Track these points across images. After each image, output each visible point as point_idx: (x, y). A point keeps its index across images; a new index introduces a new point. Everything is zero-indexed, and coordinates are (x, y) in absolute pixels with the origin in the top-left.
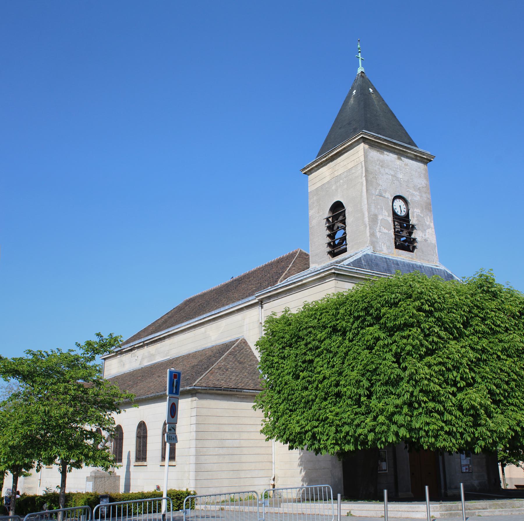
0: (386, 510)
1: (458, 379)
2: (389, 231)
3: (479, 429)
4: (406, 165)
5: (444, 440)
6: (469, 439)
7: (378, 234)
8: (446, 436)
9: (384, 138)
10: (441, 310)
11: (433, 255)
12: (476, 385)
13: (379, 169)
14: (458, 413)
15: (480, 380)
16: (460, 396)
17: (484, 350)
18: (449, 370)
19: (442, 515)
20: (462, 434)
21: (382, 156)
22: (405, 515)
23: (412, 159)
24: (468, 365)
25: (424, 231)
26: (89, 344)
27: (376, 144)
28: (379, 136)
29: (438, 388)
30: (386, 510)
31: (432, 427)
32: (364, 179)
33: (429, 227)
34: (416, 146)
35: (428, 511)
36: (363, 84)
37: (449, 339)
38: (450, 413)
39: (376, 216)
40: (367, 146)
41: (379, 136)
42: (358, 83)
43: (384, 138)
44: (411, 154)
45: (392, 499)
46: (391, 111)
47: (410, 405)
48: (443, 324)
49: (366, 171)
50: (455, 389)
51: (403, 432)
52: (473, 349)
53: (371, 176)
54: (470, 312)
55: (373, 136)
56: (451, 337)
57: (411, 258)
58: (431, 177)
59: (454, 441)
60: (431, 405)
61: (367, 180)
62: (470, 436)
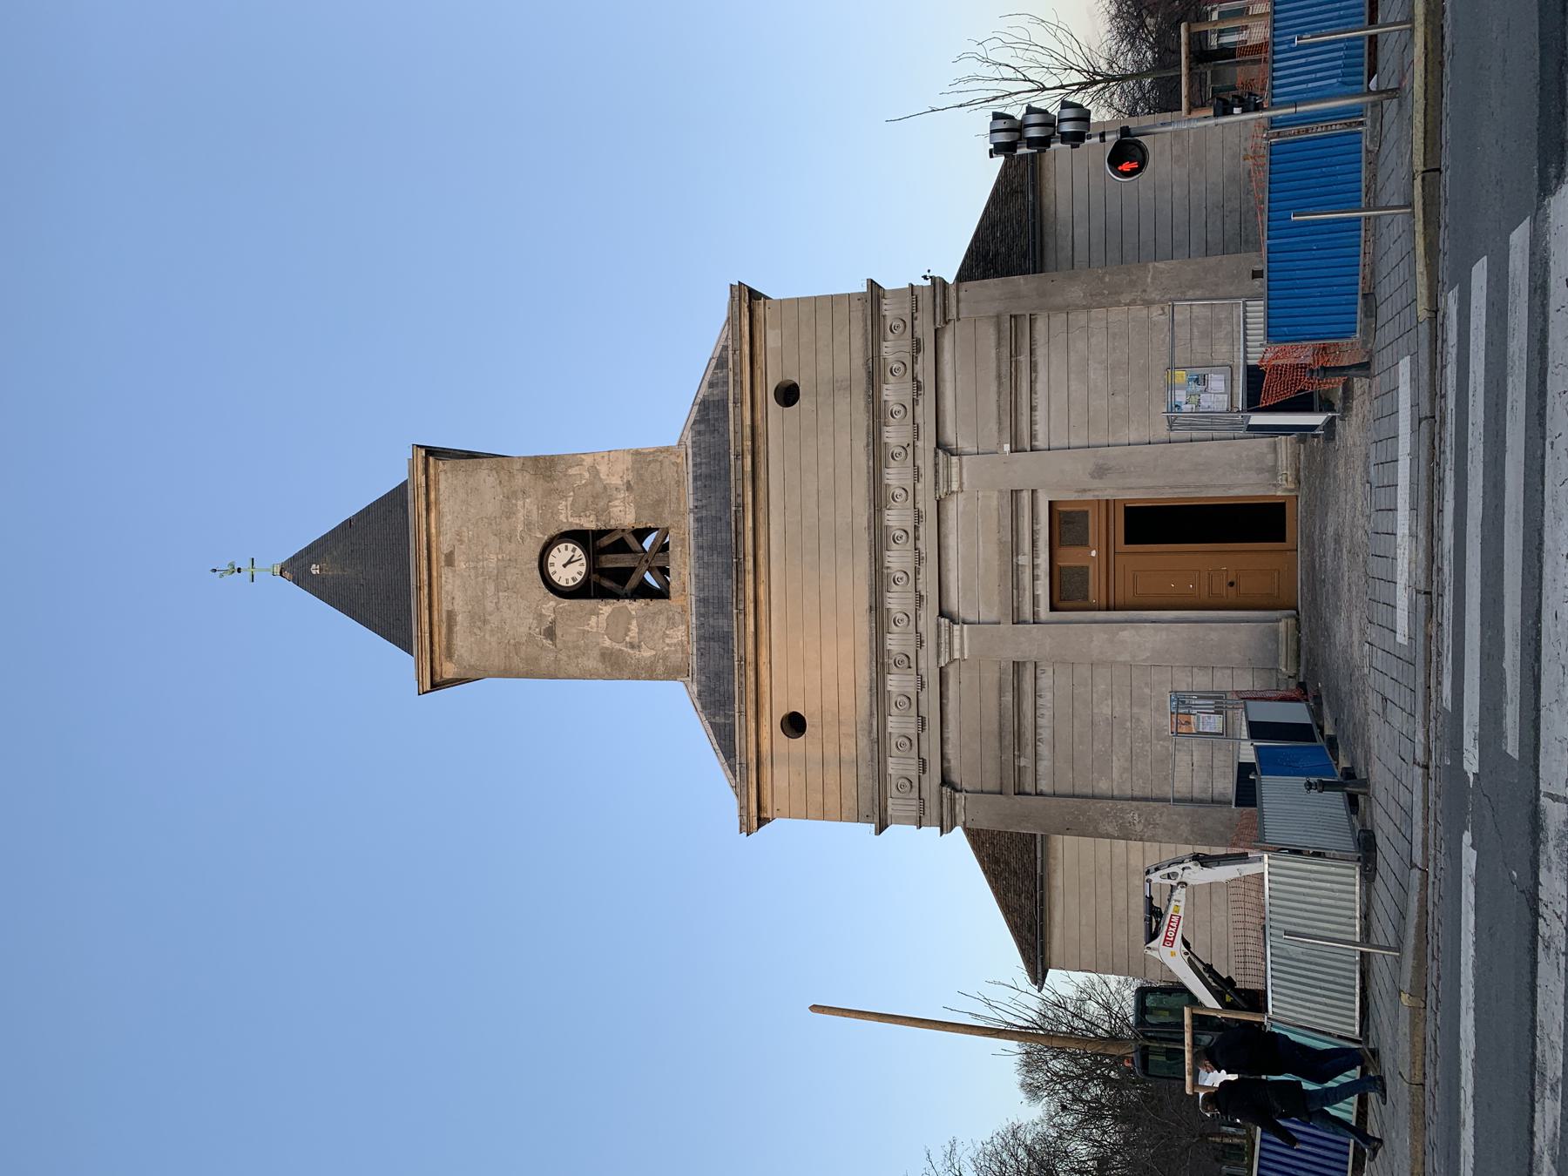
2: (630, 617)
7: (647, 653)
39: (606, 655)
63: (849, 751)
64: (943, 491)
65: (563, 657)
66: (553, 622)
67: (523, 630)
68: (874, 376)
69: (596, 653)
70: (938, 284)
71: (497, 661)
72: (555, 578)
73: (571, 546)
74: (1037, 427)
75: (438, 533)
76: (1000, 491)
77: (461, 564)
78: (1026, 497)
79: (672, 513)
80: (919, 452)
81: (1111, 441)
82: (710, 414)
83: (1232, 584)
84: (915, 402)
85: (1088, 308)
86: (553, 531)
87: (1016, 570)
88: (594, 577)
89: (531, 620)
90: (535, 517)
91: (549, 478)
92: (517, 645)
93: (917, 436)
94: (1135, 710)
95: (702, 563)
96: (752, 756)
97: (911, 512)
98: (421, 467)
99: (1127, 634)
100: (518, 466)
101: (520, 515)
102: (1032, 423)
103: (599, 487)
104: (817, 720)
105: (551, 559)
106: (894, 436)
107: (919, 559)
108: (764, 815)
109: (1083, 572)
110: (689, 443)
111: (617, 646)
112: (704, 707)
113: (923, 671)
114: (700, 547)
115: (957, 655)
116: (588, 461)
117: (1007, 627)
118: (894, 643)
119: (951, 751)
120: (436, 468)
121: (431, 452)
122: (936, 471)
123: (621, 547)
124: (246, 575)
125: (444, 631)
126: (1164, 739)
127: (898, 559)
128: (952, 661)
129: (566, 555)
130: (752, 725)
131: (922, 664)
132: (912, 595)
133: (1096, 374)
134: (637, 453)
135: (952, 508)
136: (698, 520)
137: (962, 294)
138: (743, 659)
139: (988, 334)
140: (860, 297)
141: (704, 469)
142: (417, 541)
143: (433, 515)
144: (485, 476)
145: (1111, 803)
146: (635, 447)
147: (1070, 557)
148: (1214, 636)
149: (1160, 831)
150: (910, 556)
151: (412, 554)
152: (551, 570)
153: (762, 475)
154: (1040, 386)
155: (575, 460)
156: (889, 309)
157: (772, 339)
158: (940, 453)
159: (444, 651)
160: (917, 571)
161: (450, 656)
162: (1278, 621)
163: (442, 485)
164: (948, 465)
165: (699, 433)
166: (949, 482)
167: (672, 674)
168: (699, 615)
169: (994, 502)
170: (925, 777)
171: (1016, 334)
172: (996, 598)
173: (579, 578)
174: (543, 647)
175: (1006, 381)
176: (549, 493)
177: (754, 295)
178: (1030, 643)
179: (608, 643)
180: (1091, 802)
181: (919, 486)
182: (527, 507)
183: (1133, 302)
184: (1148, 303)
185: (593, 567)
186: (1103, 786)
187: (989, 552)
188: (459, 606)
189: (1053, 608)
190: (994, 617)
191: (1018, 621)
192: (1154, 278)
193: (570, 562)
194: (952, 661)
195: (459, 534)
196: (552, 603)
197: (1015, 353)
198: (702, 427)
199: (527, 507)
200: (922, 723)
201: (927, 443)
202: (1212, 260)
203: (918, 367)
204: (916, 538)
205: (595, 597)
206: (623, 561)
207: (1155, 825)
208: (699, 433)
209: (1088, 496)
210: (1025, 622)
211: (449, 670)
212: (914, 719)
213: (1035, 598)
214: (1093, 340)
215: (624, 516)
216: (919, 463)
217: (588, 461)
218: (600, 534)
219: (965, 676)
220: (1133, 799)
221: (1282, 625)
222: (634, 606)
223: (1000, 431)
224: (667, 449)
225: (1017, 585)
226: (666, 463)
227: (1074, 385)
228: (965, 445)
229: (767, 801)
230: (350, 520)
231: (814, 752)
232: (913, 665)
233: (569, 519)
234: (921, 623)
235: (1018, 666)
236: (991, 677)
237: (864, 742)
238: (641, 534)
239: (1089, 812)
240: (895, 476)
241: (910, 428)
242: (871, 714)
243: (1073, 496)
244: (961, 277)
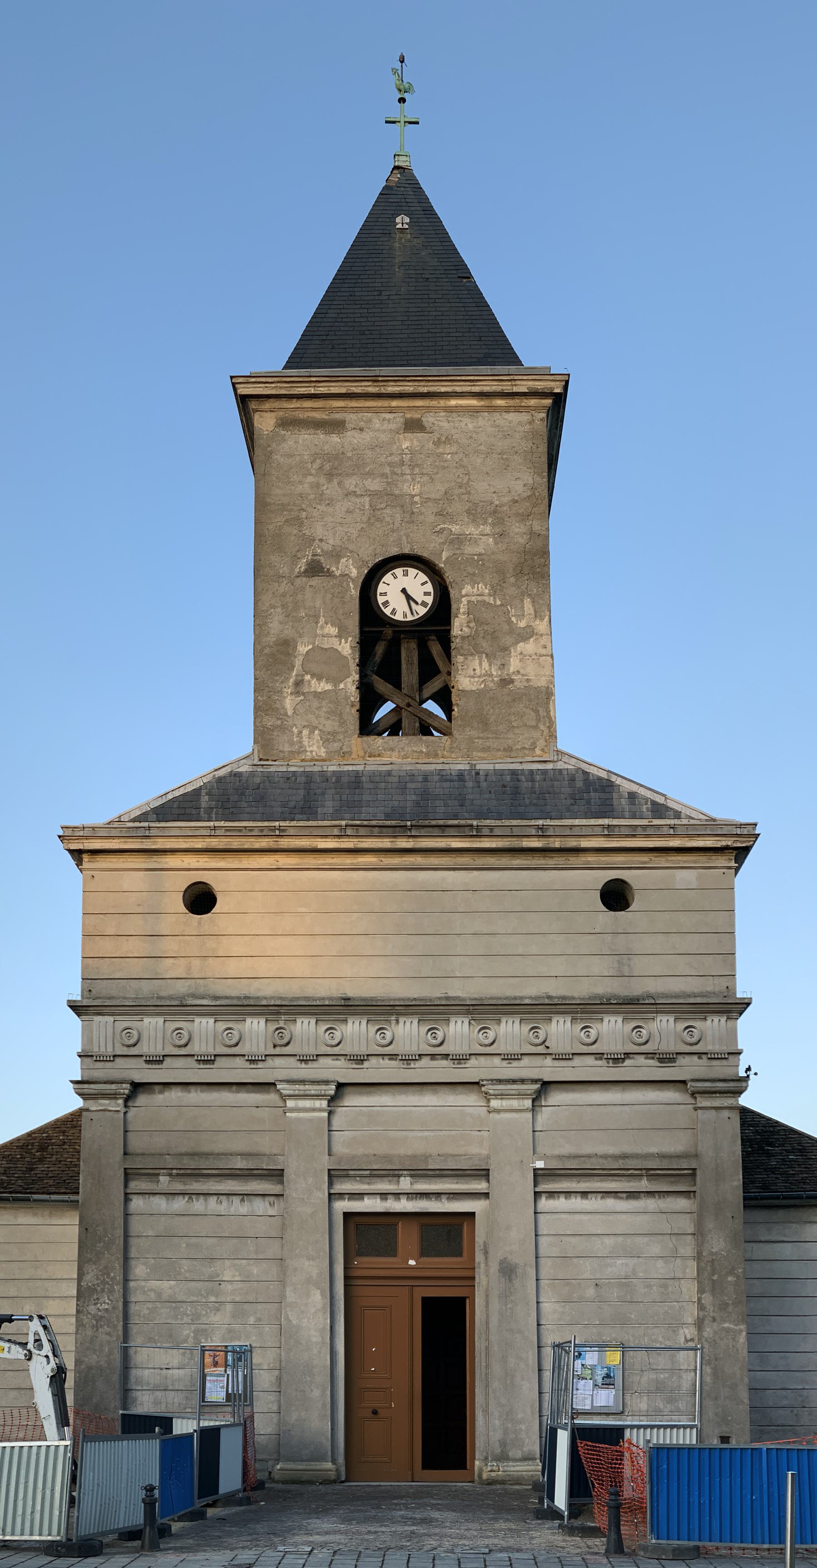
2: (336, 681)
7: (289, 703)
11: (536, 727)
13: (318, 485)
23: (474, 412)
39: (286, 646)
53: (279, 520)
57: (428, 755)
63: (172, 968)
64: (491, 1089)
65: (284, 587)
66: (329, 574)
67: (319, 531)
68: (633, 1006)
69: (289, 632)
70: (738, 1085)
71: (278, 493)
72: (388, 577)
73: (430, 600)
74: (562, 1199)
75: (449, 410)
76: (488, 1157)
77: (407, 442)
78: (480, 1186)
79: (471, 740)
80: (538, 1061)
81: (543, 1283)
82: (596, 794)
83: (375, 1412)
84: (599, 1056)
85: (699, 1257)
86: (450, 576)
87: (394, 1174)
88: (389, 632)
89: (332, 541)
90: (469, 549)
91: (519, 572)
92: (298, 522)
93: (558, 1057)
94: (229, 1307)
95: (404, 781)
96: (160, 844)
97: (466, 1050)
98: (540, 385)
99: (317, 1298)
100: (537, 527)
101: (471, 530)
102: (568, 1194)
104: (206, 929)
105: (412, 571)
106: (560, 1030)
107: (408, 1060)
108: (86, 858)
109: (390, 1250)
110: (560, 765)
111: (298, 663)
112: (220, 780)
113: (270, 1062)
114: (426, 777)
115: (290, 1103)
116: (541, 626)
117: (325, 1163)
118: (304, 1028)
119: (174, 1095)
120: (536, 409)
121: (559, 401)
122: (514, 1081)
123: (428, 669)
124: (395, 111)
125: (317, 415)
126: (195, 1338)
127: (408, 1032)
128: (284, 1098)
129: (417, 593)
130: (199, 844)
131: (278, 1061)
132: (364, 1050)
133: (620, 1266)
134: (548, 694)
135: (469, 1100)
136: (461, 775)
137: (726, 1114)
138: (282, 833)
139: (675, 1144)
140: (730, 990)
141: (525, 785)
142: (440, 379)
143: (474, 402)
144: (522, 480)
145: (120, 1278)
146: (558, 691)
147: (408, 1237)
148: (316, 1393)
149: (89, 1333)
150: (412, 1049)
151: (420, 370)
152: (399, 571)
153: (518, 862)
154: (611, 1203)
155: (543, 608)
156: (714, 1024)
157: (686, 876)
158: (537, 1086)
159: (289, 415)
160: (392, 1057)
161: (285, 423)
162: (334, 1461)
163: (513, 417)
164: (521, 1095)
165: (572, 779)
166: (501, 1096)
167: (262, 736)
168: (338, 775)
169: (474, 1150)
170: (140, 1063)
171: (674, 1175)
172: (360, 1151)
173: (387, 611)
174: (295, 558)
175: (620, 1164)
176: (500, 571)
177: (741, 854)
178: (307, 1191)
179: (303, 649)
180: (120, 1256)
181: (497, 1061)
182: (482, 539)
183: (701, 1307)
184: (699, 1324)
185: (403, 630)
186: (139, 1270)
187: (415, 1144)
188: (352, 439)
189: (347, 1216)
190: (338, 1148)
191: (333, 1176)
192: (728, 1330)
193: (409, 598)
194: (284, 1098)
195: (448, 440)
196: (354, 572)
197: (651, 1174)
198: (579, 784)
199: (482, 539)
200: (208, 1061)
201: (549, 1070)
202: (744, 1395)
203: (641, 1060)
204: (433, 1056)
205: (362, 632)
206: (409, 673)
207: (96, 1328)
208: (572, 779)
209: (479, 1257)
210: (331, 1184)
211: (265, 422)
212: (211, 1051)
213: (359, 1196)
214: (660, 1263)
215: (469, 675)
216: (526, 1061)
217: (541, 626)
218: (446, 641)
219: (264, 1113)
220: (126, 1304)
221: (329, 1465)
222: (350, 686)
223: (560, 1157)
224: (553, 736)
225: (375, 1175)
226: (536, 734)
227: (609, 1241)
228: (545, 1116)
229: (103, 862)
230: (469, 277)
231: (166, 925)
232: (278, 1051)
233: (467, 595)
234: (328, 1061)
235: (278, 1175)
236: (265, 1144)
237: (181, 988)
238: (444, 698)
239: (107, 1254)
240: (510, 1031)
241: (569, 1050)
242: (216, 998)
243: (480, 1239)
244: (745, 1112)
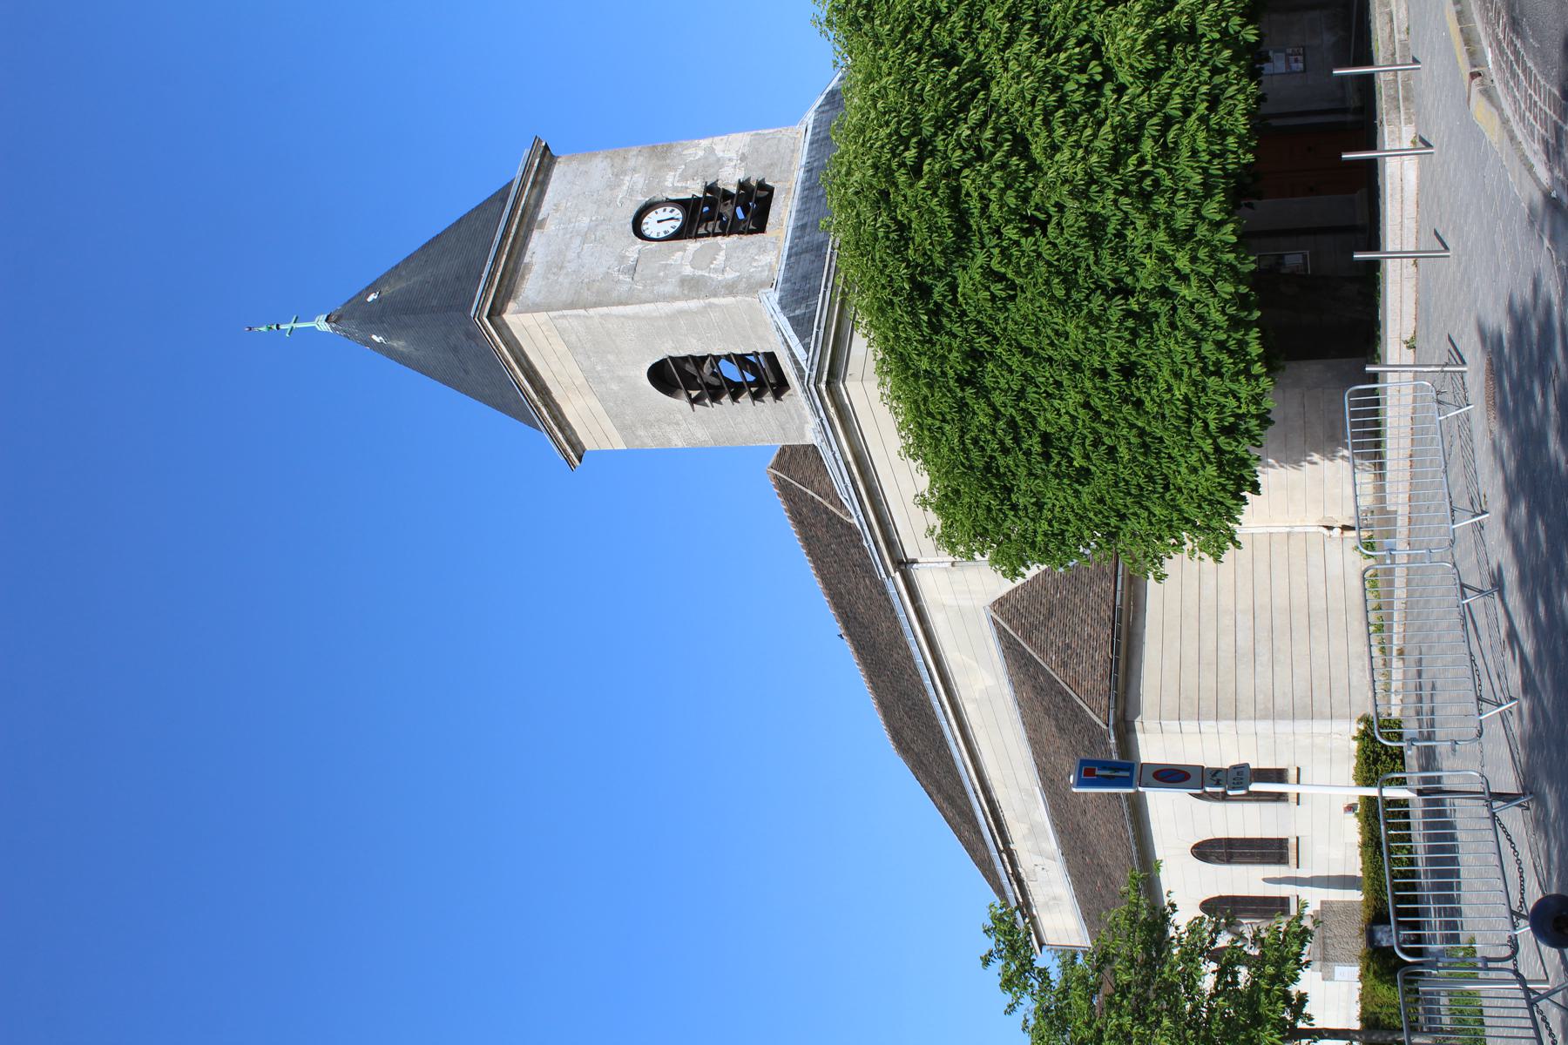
0: (1401, 255)
1: (1083, 79)
2: (719, 248)
3: (1201, 29)
4: (557, 207)
5: (1230, 113)
6: (1227, 53)
7: (730, 275)
8: (1222, 110)
9: (489, 262)
10: (916, 120)
12: (1096, 37)
13: (567, 274)
14: (1166, 79)
15: (1084, 26)
16: (1124, 76)
17: (1013, 16)
18: (1062, 102)
19: (1409, 121)
20: (1215, 71)
21: (535, 268)
22: (1411, 209)
23: (542, 193)
24: (1048, 55)
25: (720, 163)
26: (1008, 984)
27: (506, 282)
28: (485, 275)
29: (1106, 128)
30: (1401, 255)
31: (1201, 145)
32: (592, 311)
33: (711, 150)
34: (511, 183)
35: (1400, 153)
36: (356, 316)
37: (986, 100)
38: (1165, 100)
39: (684, 281)
40: (511, 306)
41: (485, 275)
42: (353, 329)
43: (489, 262)
44: (529, 196)
45: (1373, 239)
46: (424, 247)
47: (1146, 197)
48: (950, 115)
49: (572, 305)
50: (1108, 88)
51: (1212, 210)
52: (1009, 43)
54: (919, 49)
55: (486, 290)
56: (981, 95)
58: (587, 147)
59: (1231, 91)
60: (1147, 147)
61: (595, 305)
62: (1219, 52)
69: (674, 280)
103: (712, 159)
